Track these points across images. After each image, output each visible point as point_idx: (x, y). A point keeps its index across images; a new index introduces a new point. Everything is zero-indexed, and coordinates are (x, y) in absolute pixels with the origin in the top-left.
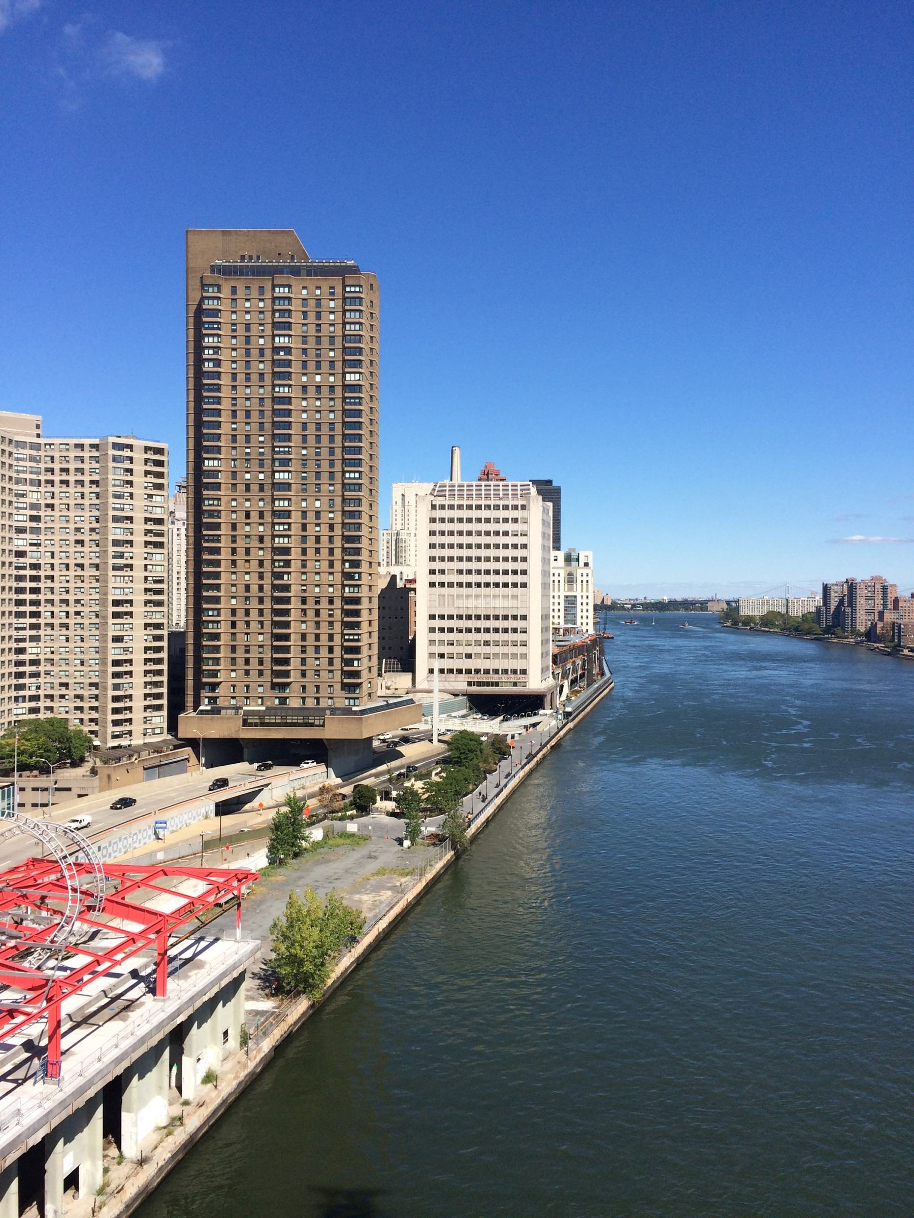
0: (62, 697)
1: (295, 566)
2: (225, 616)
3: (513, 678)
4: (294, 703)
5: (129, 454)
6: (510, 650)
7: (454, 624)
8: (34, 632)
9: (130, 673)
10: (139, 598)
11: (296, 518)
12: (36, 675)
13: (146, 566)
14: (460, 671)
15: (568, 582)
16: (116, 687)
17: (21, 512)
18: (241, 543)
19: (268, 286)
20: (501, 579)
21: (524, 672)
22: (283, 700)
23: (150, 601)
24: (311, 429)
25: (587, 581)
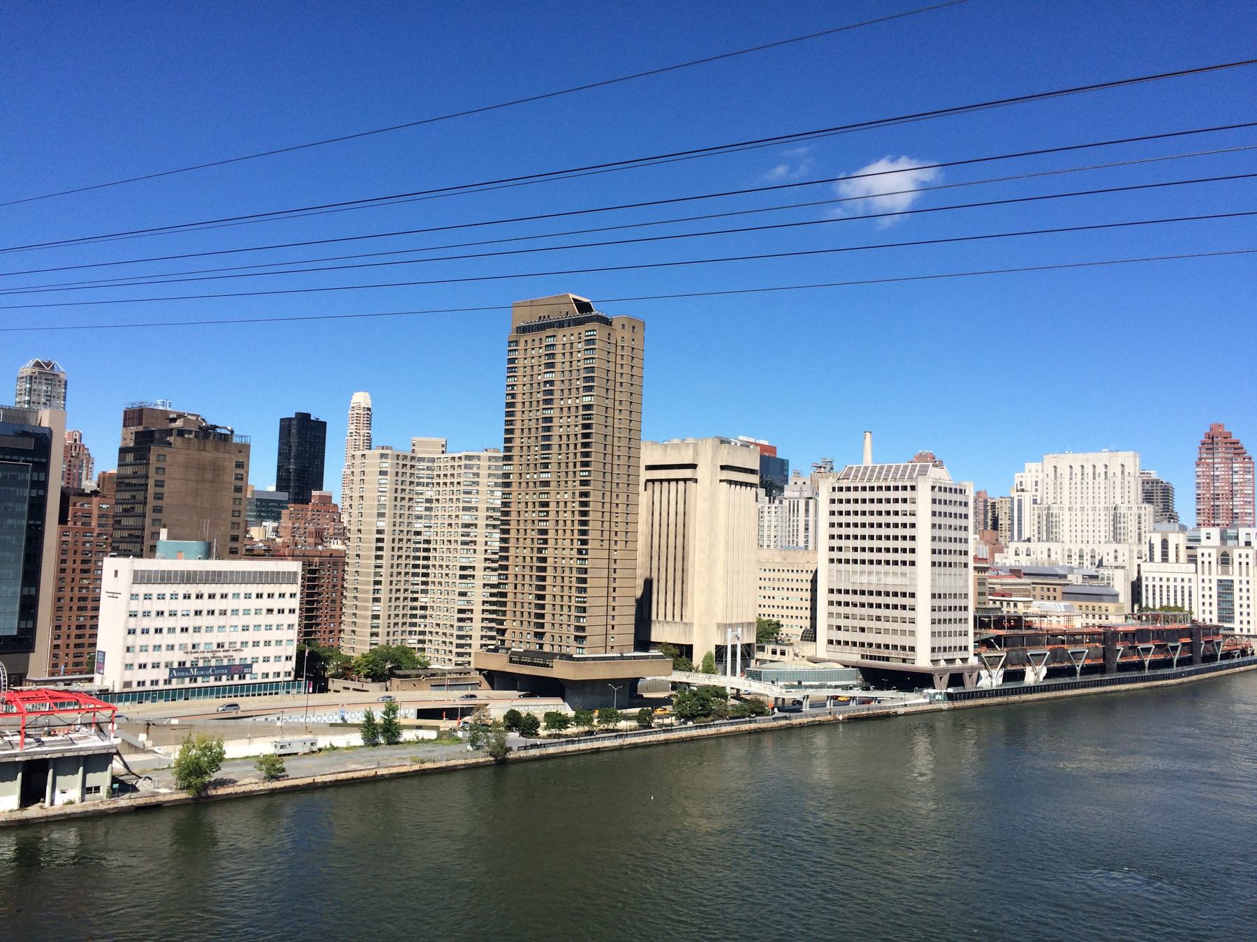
0: (437, 633)
1: (551, 543)
3: (902, 654)
4: (547, 649)
5: (477, 462)
7: (850, 598)
8: (424, 587)
9: (471, 619)
10: (480, 565)
11: (553, 506)
12: (424, 617)
13: (486, 543)
14: (854, 644)
15: (1222, 563)
16: (460, 628)
17: (420, 504)
18: (522, 526)
19: (544, 338)
21: (912, 649)
22: (541, 646)
23: (489, 568)
24: (564, 438)
25: (1247, 564)
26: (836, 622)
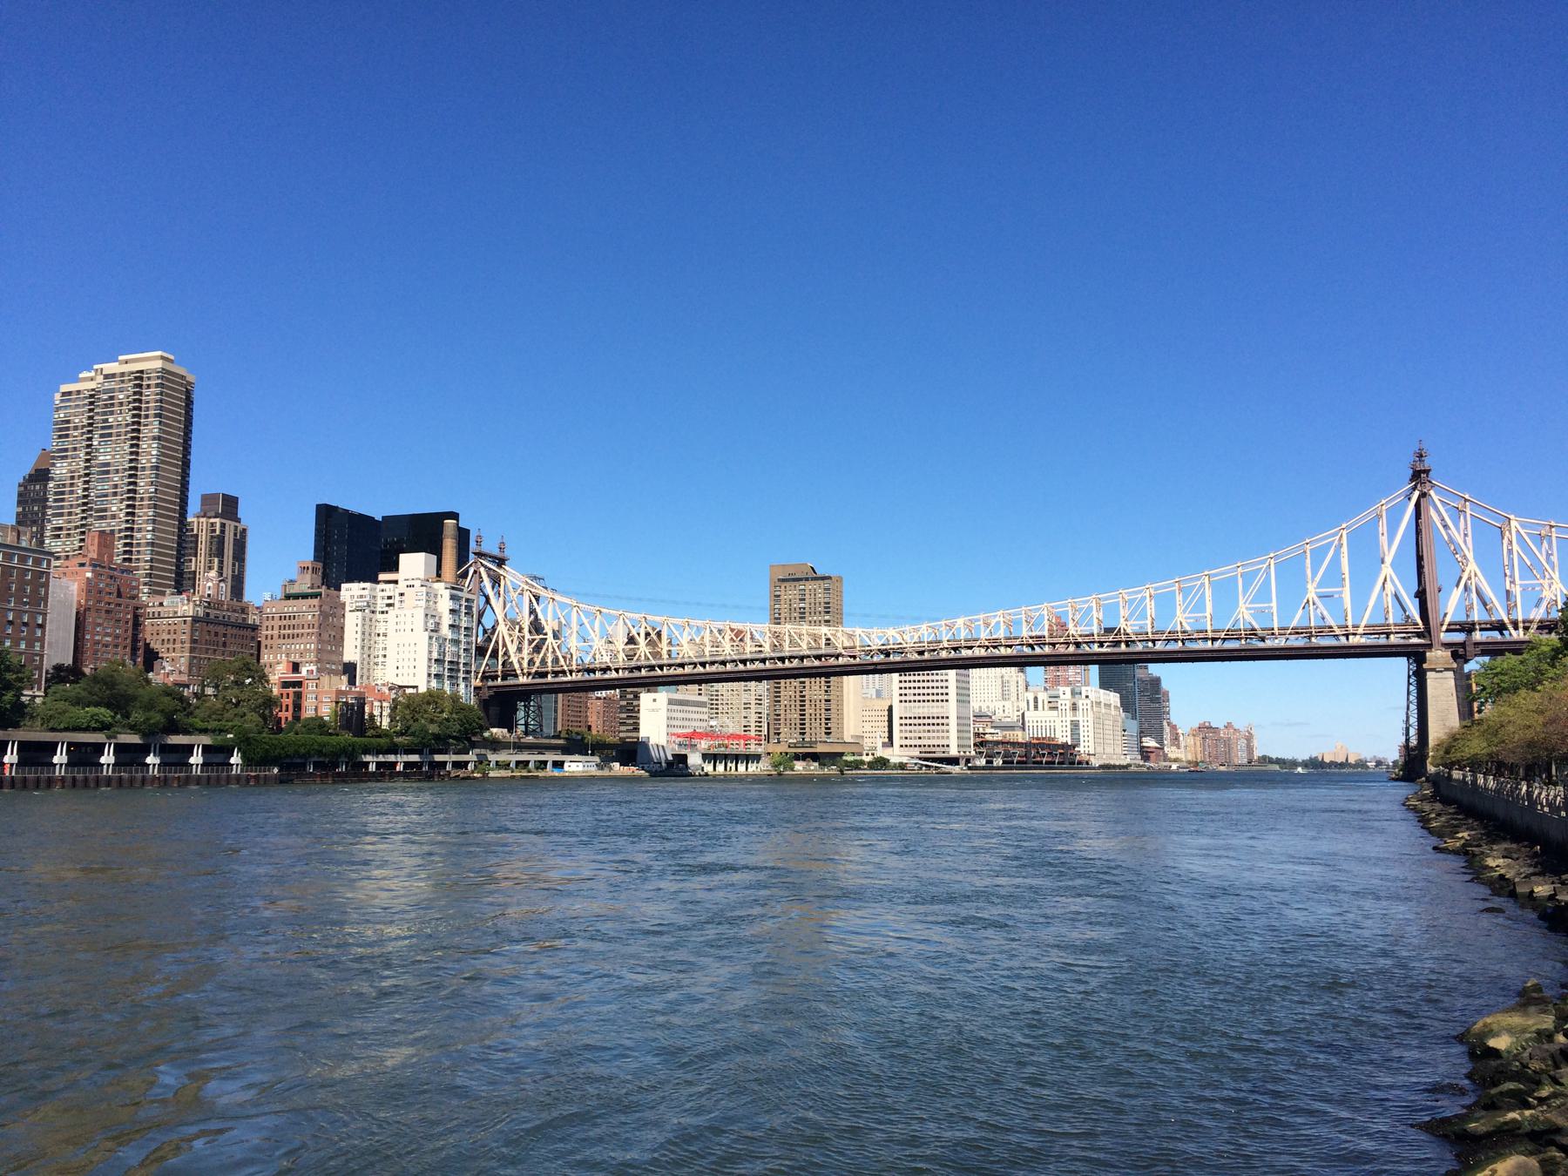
2: (783, 707)
6: (941, 734)
7: (912, 721)
10: (753, 702)
20: (935, 698)
21: (948, 746)
26: (904, 735)
